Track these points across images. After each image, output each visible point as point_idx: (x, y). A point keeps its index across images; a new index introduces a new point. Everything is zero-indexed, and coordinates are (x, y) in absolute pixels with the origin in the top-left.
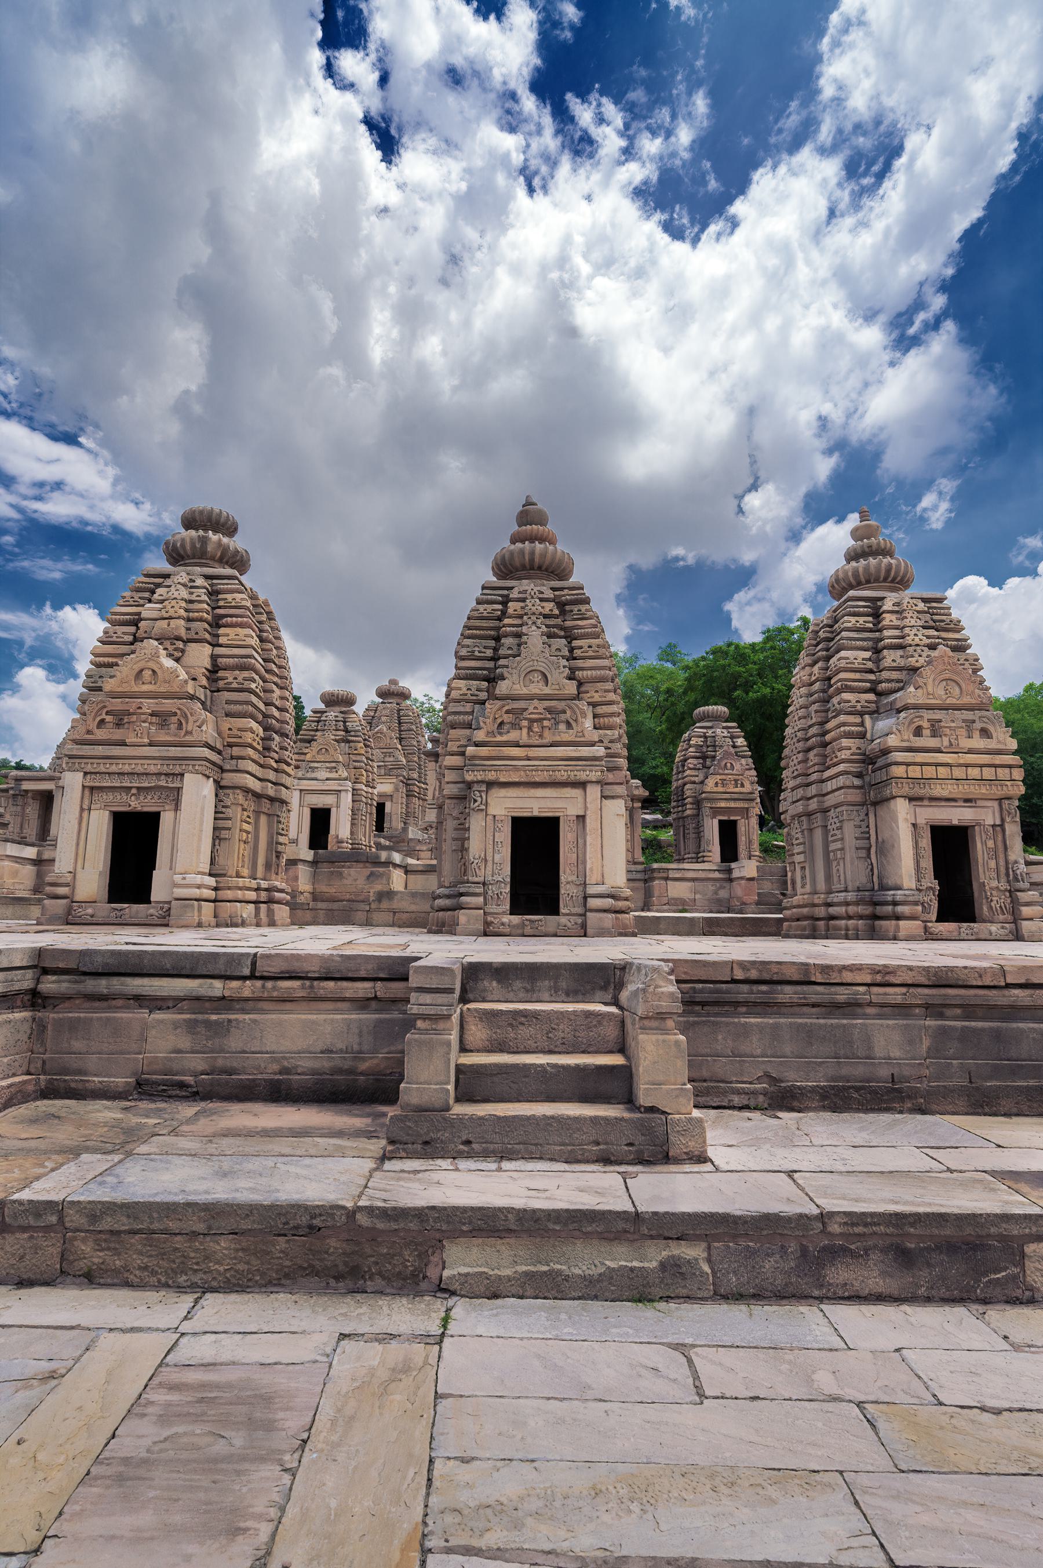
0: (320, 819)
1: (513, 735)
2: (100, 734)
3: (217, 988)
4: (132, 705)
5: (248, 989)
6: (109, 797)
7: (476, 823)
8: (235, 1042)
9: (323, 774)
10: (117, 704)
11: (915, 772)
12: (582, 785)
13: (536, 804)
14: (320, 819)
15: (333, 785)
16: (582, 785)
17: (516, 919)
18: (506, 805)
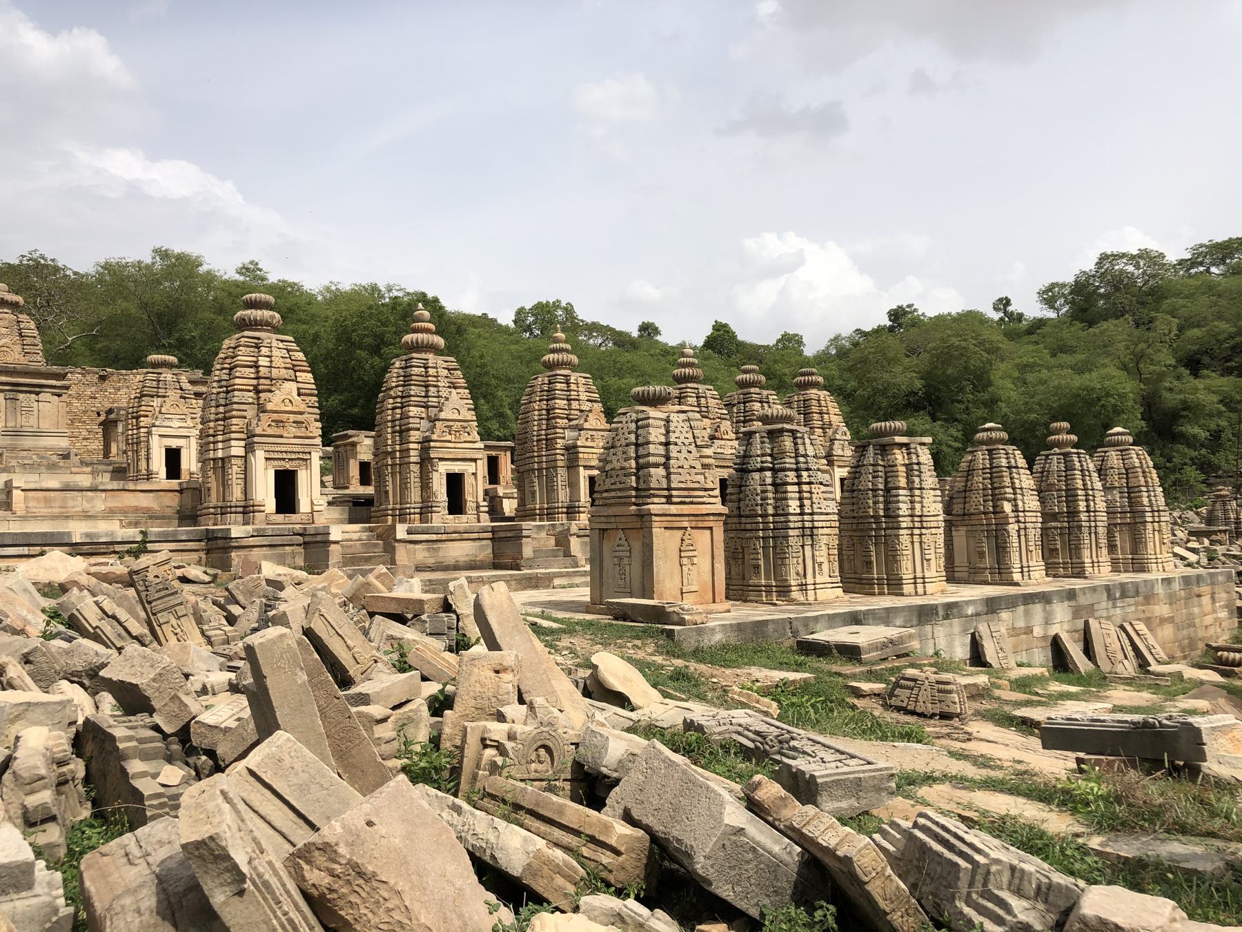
0: (173, 457)
1: (448, 438)
2: (270, 431)
3: (434, 537)
4: (284, 417)
5: (444, 537)
6: (276, 463)
7: (435, 476)
8: (441, 554)
9: (176, 424)
10: (275, 416)
11: (586, 456)
12: (475, 460)
13: (456, 468)
14: (173, 457)
15: (184, 432)
16: (475, 460)
17: (451, 517)
18: (444, 468)
